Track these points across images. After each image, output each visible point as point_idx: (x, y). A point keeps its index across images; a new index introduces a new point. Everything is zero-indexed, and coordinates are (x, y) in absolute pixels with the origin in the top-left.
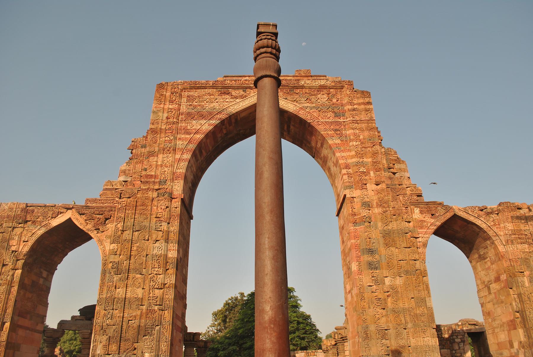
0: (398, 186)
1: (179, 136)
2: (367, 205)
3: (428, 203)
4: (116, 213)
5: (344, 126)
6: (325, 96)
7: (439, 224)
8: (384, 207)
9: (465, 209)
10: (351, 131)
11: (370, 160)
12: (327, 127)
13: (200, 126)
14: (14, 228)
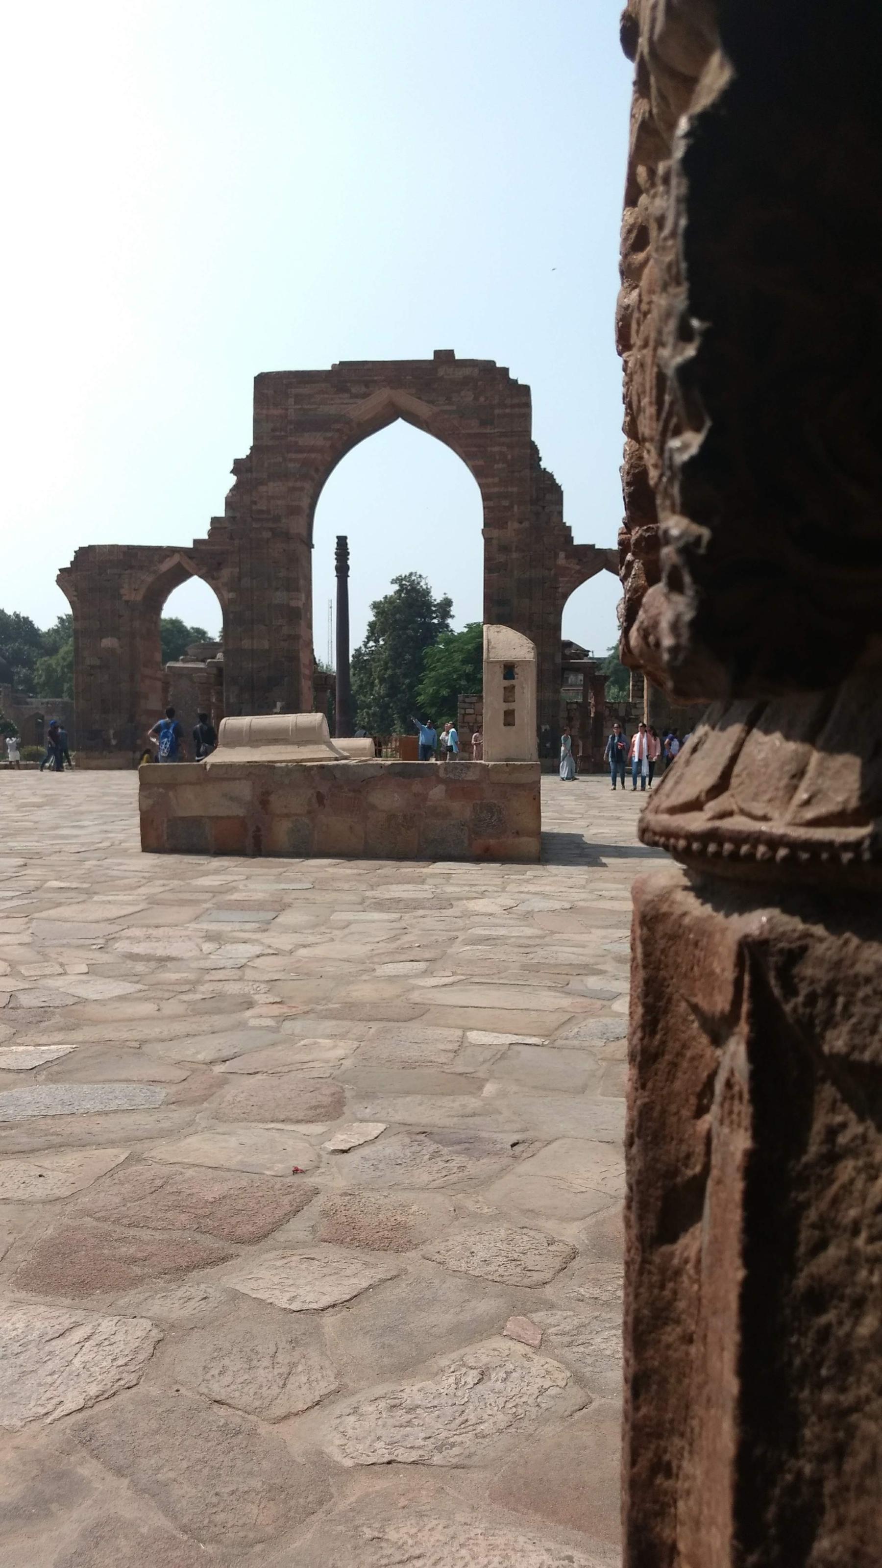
2: (504, 548)
10: (496, 449)
11: (515, 489)
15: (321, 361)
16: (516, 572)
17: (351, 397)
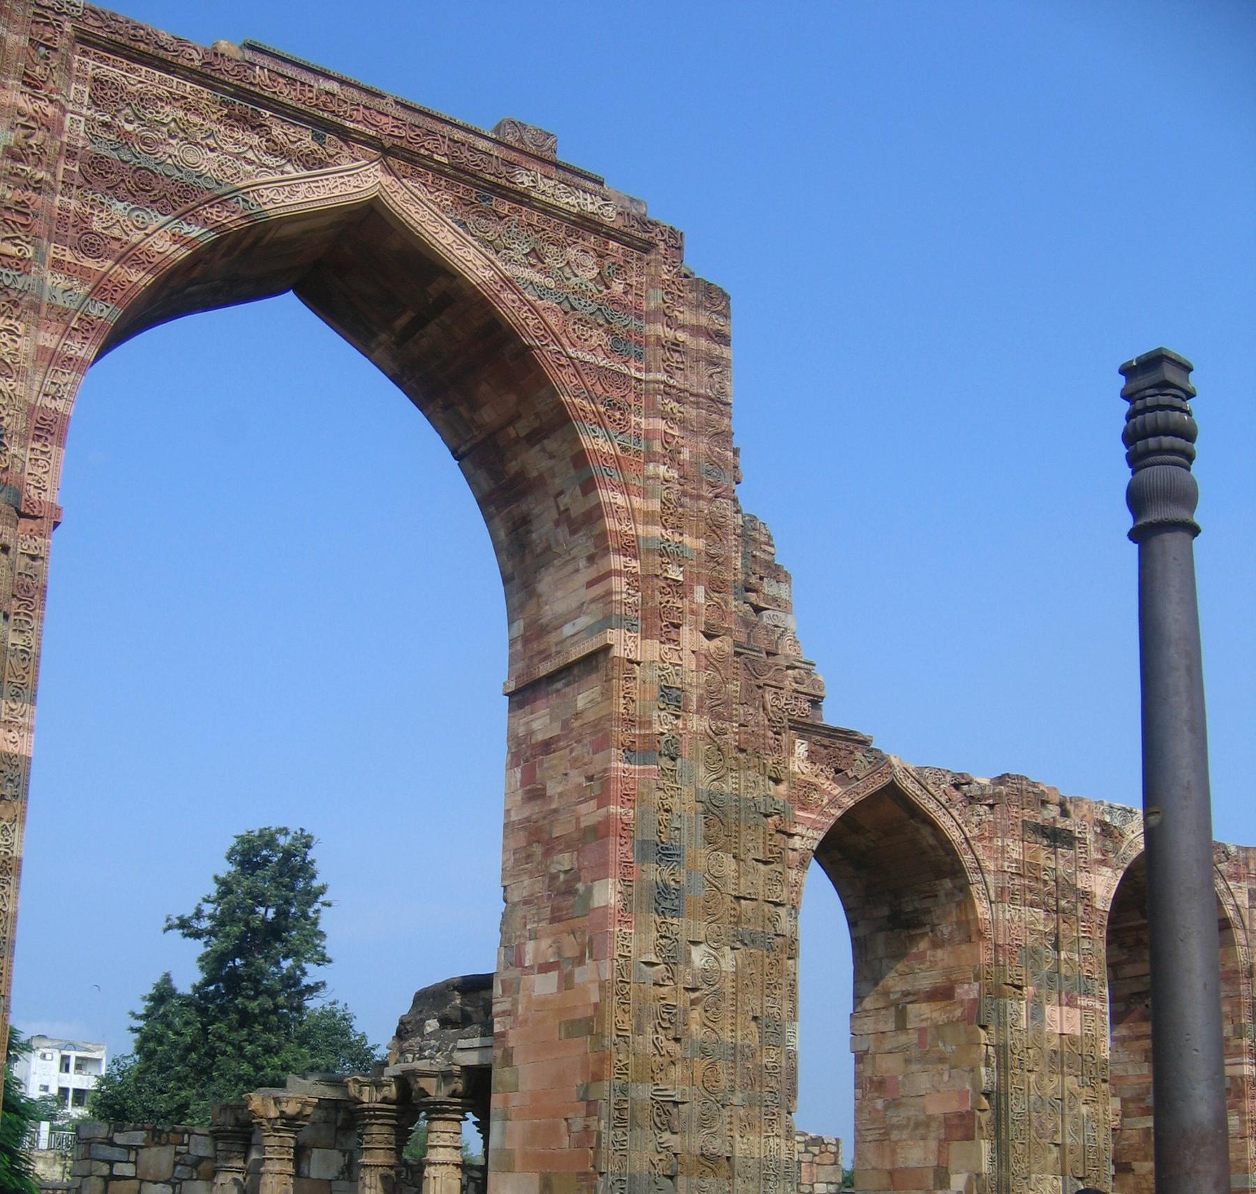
0: (764, 655)
1: (52, 250)
2: (672, 697)
3: (833, 733)
5: (638, 396)
7: (849, 802)
8: (718, 717)
9: (920, 770)
11: (700, 544)
13: (141, 235)
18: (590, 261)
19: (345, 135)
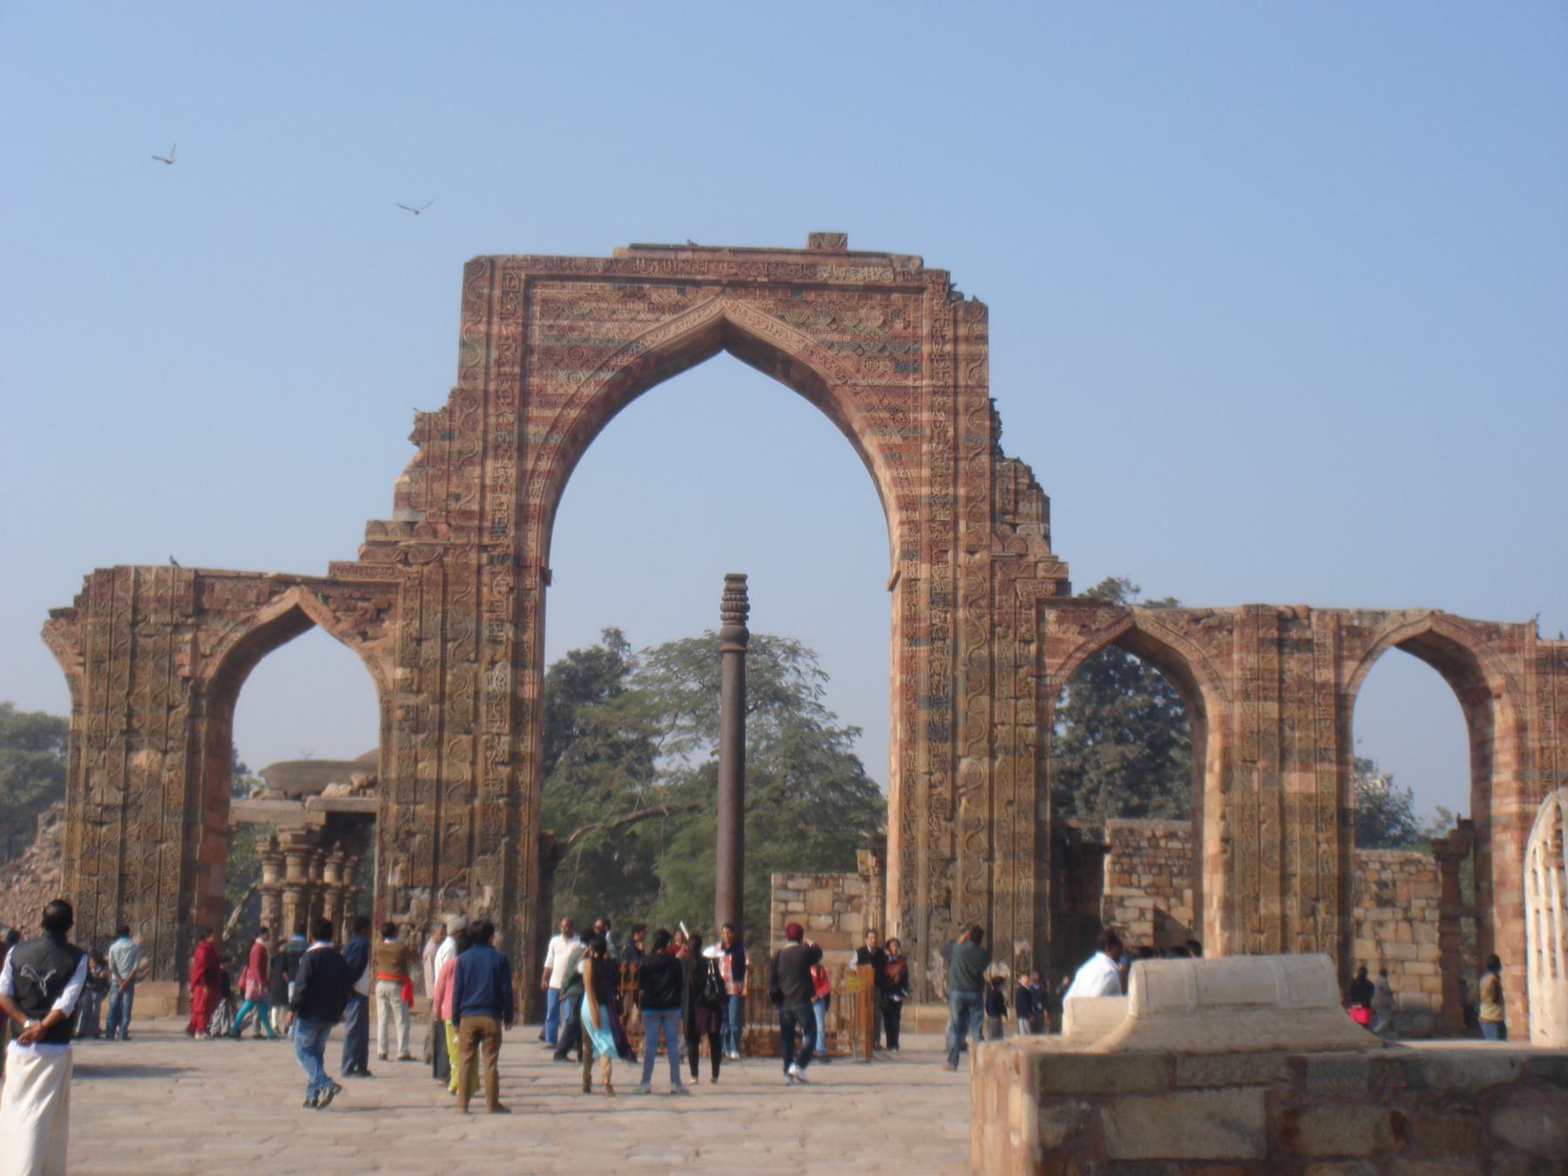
3: (1080, 602)
4: (400, 599)
5: (915, 399)
6: (877, 313)
8: (979, 606)
12: (875, 400)
14: (177, 628)
15: (597, 238)
16: (962, 646)
17: (651, 310)
18: (877, 313)
19: (697, 284)
